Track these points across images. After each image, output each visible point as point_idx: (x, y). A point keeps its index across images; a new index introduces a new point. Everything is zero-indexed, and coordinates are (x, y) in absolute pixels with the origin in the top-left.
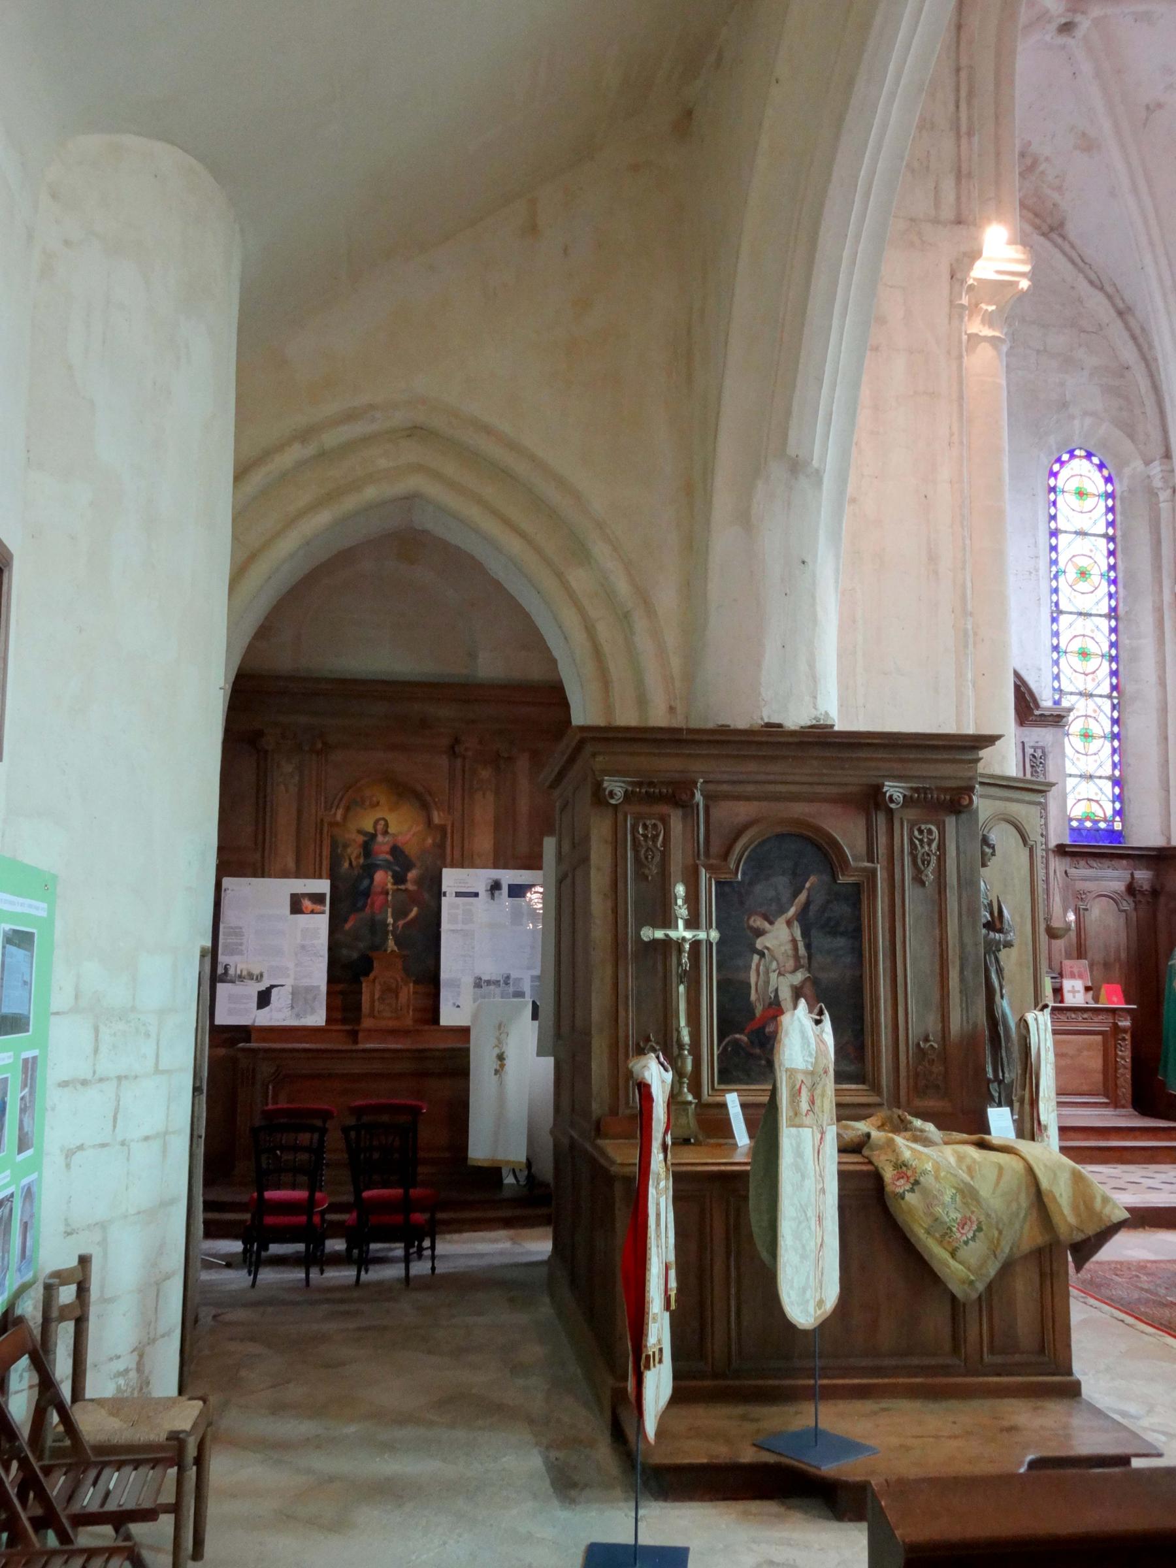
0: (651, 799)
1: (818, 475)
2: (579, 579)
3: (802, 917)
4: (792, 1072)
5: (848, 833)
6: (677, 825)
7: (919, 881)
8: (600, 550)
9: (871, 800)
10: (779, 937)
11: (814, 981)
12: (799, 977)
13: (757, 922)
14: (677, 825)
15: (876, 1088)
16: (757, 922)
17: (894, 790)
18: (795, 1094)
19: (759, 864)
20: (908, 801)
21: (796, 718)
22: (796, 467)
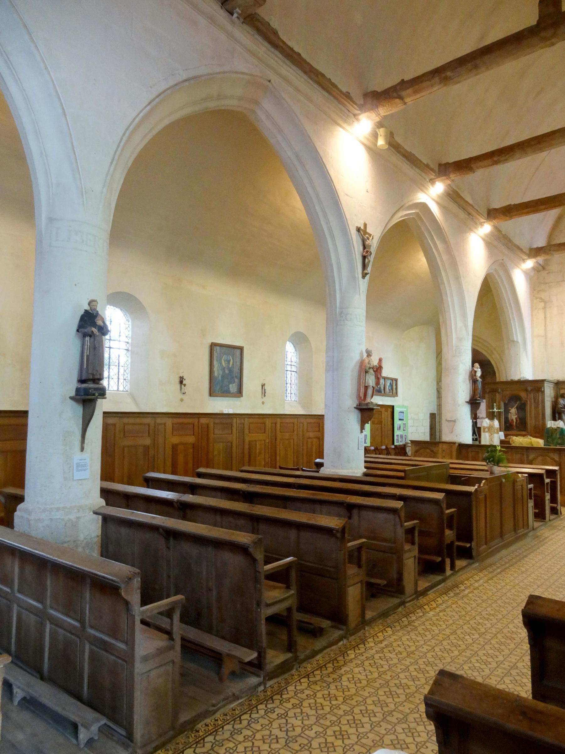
0: (493, 392)
1: (517, 342)
2: (493, 356)
3: (517, 408)
4: (484, 427)
5: (523, 395)
6: (497, 395)
7: (535, 402)
8: (495, 352)
9: (526, 390)
10: (513, 411)
11: (518, 417)
12: (516, 416)
13: (510, 408)
14: (497, 395)
15: (528, 432)
16: (510, 408)
17: (529, 389)
18: (484, 429)
19: (509, 401)
20: (532, 390)
21: (516, 378)
22: (513, 341)
